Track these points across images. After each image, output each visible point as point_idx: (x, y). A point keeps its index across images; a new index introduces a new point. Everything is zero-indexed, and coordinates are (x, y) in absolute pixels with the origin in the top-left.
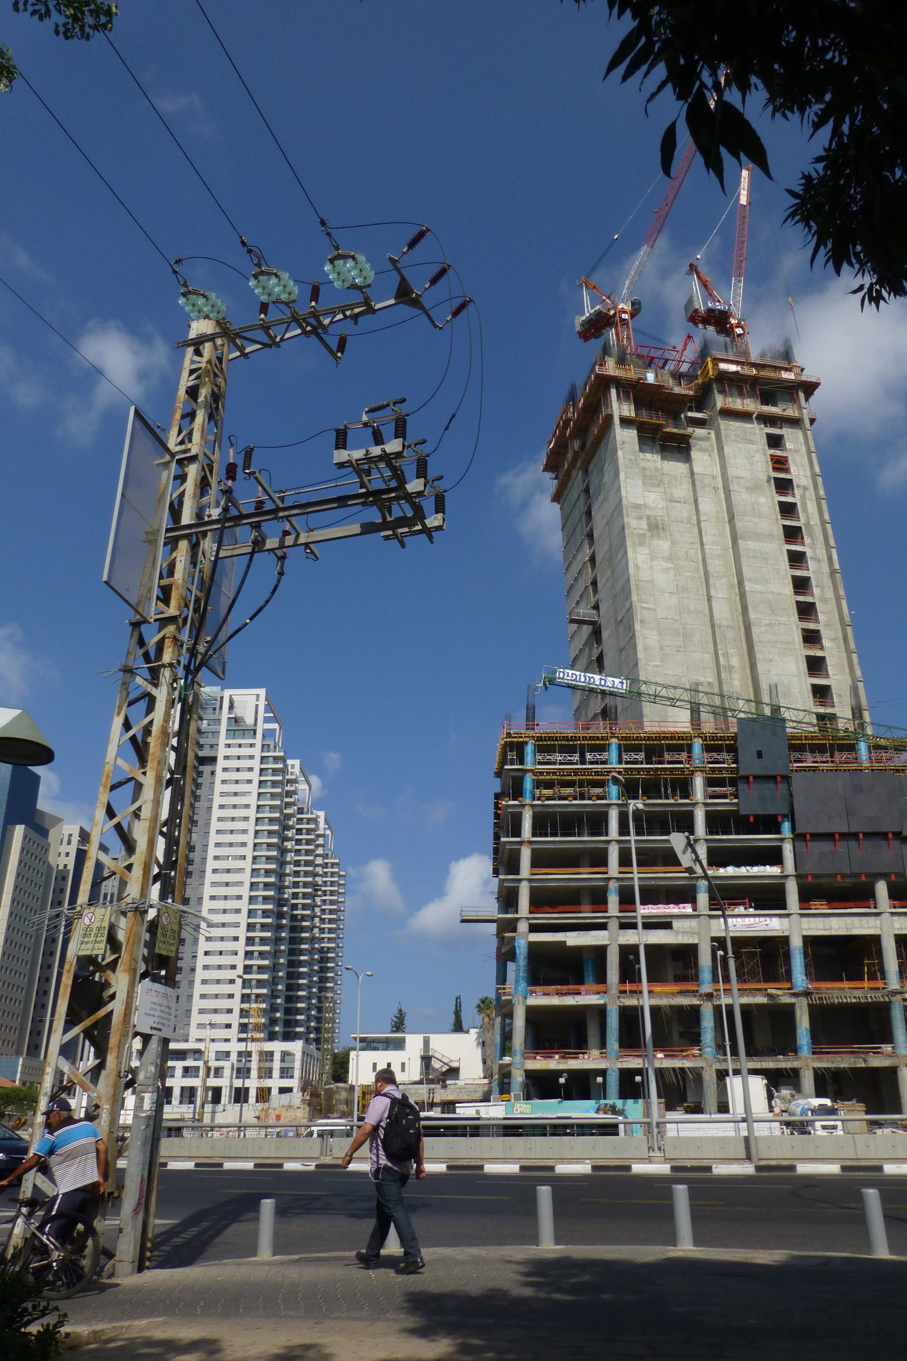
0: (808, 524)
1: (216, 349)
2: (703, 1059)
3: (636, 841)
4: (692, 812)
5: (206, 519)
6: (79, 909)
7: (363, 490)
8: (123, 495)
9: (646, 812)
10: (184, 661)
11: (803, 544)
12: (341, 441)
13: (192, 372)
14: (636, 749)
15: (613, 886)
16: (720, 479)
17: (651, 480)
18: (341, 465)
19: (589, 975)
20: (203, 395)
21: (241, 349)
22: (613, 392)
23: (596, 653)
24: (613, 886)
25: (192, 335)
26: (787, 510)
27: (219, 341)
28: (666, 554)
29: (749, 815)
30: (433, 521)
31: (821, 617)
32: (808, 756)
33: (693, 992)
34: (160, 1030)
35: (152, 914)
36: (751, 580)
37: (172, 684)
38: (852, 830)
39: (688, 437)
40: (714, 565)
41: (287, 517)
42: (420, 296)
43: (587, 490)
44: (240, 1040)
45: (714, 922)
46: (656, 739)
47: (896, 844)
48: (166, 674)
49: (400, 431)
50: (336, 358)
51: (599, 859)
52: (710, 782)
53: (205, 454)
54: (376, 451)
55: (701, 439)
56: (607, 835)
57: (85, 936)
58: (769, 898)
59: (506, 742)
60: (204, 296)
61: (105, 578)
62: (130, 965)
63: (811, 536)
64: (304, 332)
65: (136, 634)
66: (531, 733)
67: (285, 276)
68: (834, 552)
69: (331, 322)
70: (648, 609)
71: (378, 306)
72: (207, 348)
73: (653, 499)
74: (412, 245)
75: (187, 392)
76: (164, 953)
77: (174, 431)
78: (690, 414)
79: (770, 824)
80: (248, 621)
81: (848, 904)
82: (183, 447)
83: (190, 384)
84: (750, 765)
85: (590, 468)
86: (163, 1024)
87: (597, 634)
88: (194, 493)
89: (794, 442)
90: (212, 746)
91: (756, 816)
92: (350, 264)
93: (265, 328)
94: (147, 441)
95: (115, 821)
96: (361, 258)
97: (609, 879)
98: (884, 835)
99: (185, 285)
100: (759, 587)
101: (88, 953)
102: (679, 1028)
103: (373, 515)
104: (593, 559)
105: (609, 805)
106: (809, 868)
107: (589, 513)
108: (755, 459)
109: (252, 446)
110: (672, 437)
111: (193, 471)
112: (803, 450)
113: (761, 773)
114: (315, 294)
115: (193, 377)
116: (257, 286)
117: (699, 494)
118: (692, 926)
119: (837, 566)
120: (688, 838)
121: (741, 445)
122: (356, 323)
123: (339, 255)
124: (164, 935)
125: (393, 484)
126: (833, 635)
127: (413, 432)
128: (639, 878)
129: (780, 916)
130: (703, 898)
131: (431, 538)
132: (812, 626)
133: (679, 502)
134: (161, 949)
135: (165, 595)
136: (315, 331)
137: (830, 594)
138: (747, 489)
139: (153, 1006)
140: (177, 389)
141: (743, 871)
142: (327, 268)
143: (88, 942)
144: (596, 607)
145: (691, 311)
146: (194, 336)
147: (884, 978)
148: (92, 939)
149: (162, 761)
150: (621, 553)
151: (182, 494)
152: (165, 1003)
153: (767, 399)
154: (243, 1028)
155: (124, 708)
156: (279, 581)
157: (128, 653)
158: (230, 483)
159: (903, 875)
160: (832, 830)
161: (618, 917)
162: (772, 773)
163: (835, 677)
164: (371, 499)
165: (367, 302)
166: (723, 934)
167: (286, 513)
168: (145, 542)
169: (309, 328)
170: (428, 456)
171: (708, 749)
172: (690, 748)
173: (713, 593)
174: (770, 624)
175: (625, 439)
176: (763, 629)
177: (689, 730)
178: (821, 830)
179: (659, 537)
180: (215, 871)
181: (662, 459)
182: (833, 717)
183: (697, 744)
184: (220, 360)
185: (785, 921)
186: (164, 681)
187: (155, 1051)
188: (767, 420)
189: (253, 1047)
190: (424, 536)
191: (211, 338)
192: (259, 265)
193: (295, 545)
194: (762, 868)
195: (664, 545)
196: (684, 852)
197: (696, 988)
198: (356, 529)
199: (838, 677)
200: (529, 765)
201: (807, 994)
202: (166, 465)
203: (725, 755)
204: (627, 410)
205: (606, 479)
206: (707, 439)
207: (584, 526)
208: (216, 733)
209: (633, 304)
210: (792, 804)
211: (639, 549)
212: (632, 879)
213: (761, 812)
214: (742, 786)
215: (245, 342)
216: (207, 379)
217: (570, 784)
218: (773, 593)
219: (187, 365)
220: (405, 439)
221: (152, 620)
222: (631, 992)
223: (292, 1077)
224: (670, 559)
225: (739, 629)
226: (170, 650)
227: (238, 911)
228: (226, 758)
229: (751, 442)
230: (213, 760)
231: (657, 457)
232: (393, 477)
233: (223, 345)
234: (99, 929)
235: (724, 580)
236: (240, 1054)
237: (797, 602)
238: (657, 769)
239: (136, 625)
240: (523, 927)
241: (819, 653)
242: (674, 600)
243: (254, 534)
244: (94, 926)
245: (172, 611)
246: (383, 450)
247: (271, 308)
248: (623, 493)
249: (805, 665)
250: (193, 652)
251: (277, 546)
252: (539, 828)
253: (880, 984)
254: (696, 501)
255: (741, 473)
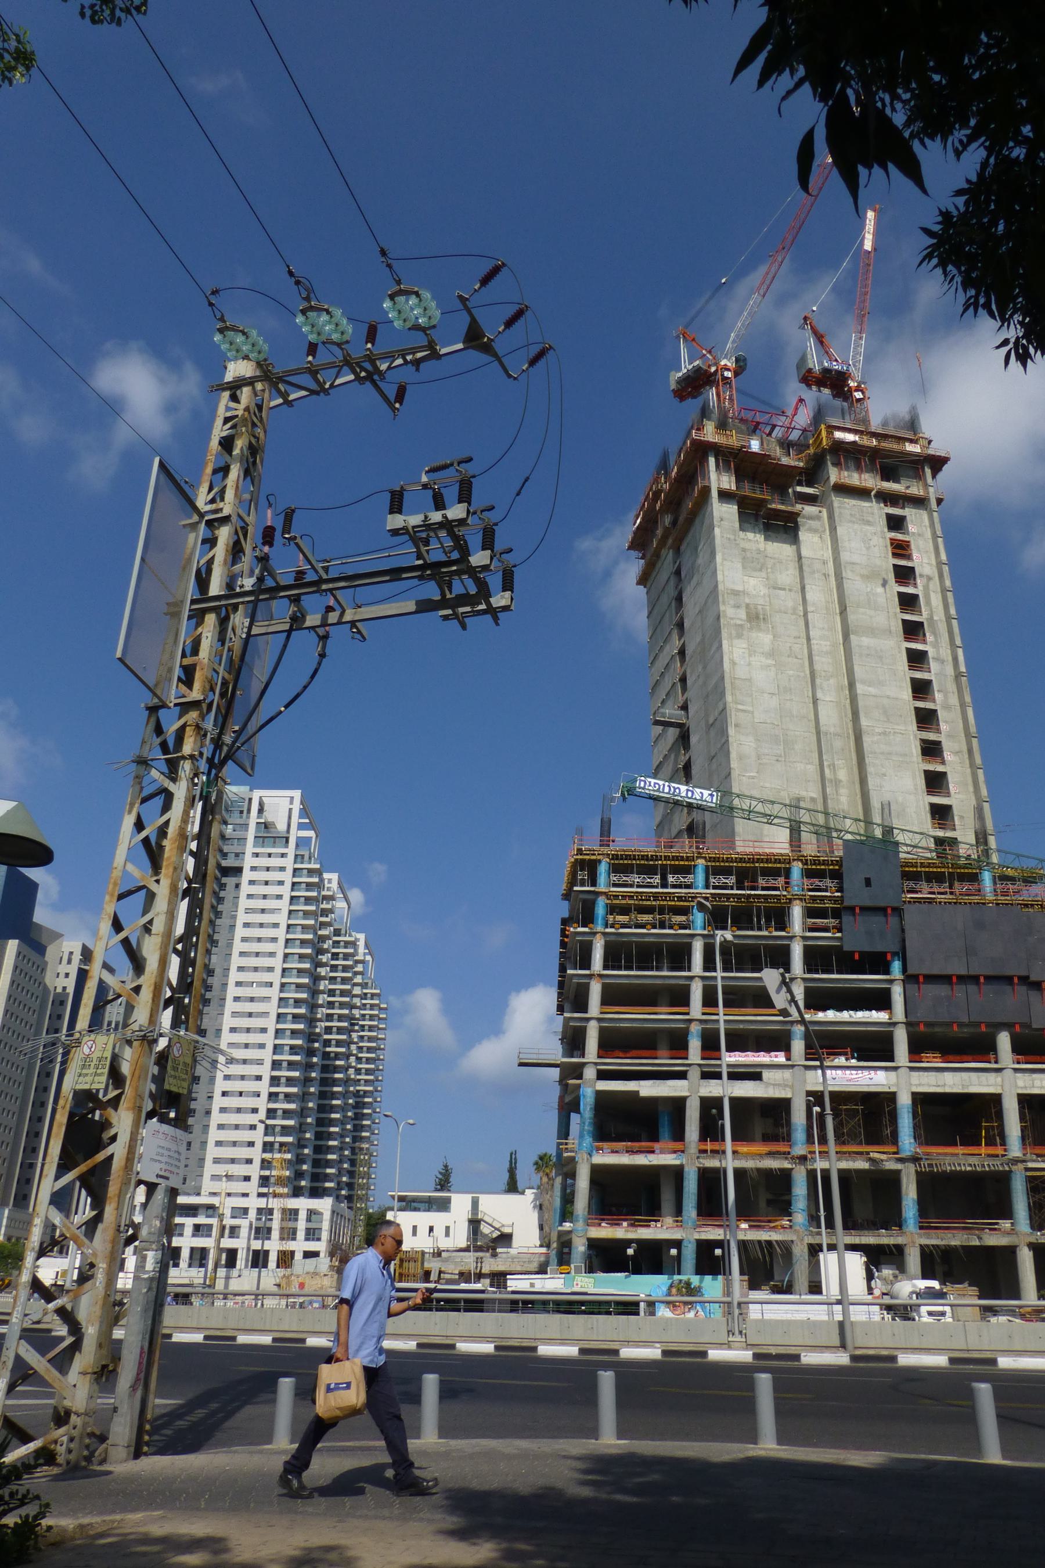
0: (931, 618)
1: (256, 395)
2: (793, 1230)
3: (723, 978)
4: (789, 945)
5: (238, 590)
6: (77, 1035)
7: (420, 562)
8: (143, 559)
9: (735, 945)
10: (207, 752)
11: (924, 642)
12: (397, 504)
13: (227, 420)
14: (726, 872)
15: (695, 1029)
16: (831, 564)
17: (752, 563)
18: (395, 532)
19: (665, 1131)
20: (239, 447)
21: (284, 395)
22: (712, 461)
23: (683, 759)
24: (695, 1029)
25: (229, 377)
26: (908, 602)
27: (259, 386)
28: (767, 649)
29: (853, 953)
30: (500, 599)
31: (943, 727)
32: (924, 886)
33: (784, 1153)
34: (167, 1178)
35: (163, 1043)
36: (863, 682)
37: (192, 779)
38: (972, 973)
39: (798, 514)
40: (822, 663)
41: (331, 590)
42: (492, 340)
43: (678, 573)
44: (260, 1195)
45: (810, 1074)
46: (749, 861)
47: (1021, 990)
48: (186, 767)
49: (465, 495)
50: (394, 409)
51: (680, 997)
52: (810, 913)
53: (239, 516)
54: (436, 517)
55: (811, 518)
56: (689, 970)
57: (83, 1067)
58: (873, 1048)
59: (576, 860)
60: (244, 333)
61: (119, 654)
62: (135, 1103)
63: (934, 633)
64: (358, 378)
65: (153, 719)
66: (606, 850)
67: (338, 312)
68: (960, 652)
69: (389, 368)
70: (743, 711)
71: (443, 351)
72: (245, 394)
73: (754, 585)
74: (485, 281)
75: (220, 443)
76: (174, 1089)
77: (204, 489)
78: (799, 489)
79: (878, 963)
80: (283, 709)
81: (965, 1057)
82: (213, 506)
83: (224, 434)
84: (856, 895)
85: (682, 548)
86: (171, 1172)
87: (684, 738)
88: (225, 561)
89: (917, 522)
90: (237, 855)
91: (860, 952)
92: (413, 301)
93: (313, 372)
94: (171, 497)
95: (122, 935)
96: (426, 295)
97: (690, 1021)
98: (1008, 980)
99: (222, 319)
100: (872, 690)
101: (87, 1087)
102: (767, 1194)
103: (431, 591)
104: (682, 652)
105: (693, 936)
106: (921, 1015)
107: (679, 599)
108: (872, 543)
109: (293, 507)
110: (777, 514)
111: (224, 534)
112: (928, 534)
113: (868, 903)
114: (372, 334)
115: (229, 425)
116: (305, 324)
117: (806, 581)
118: (784, 1078)
119: (963, 669)
120: (782, 975)
121: (856, 526)
122: (417, 370)
123: (400, 290)
124: (175, 1069)
125: (455, 555)
126: (956, 747)
127: (479, 499)
128: (725, 1021)
130: (798, 1046)
131: (496, 620)
132: (932, 736)
133: (784, 589)
134: (171, 1085)
135: (188, 677)
136: (369, 377)
137: (954, 700)
138: (862, 576)
139: (161, 1151)
140: (210, 439)
141: (845, 1016)
142: (387, 304)
143: (87, 1075)
144: (685, 707)
145: (804, 371)
146: (231, 379)
147: (1003, 1143)
148: (92, 1070)
149: (179, 868)
150: (714, 648)
151: (211, 562)
152: (174, 1147)
153: (888, 474)
154: (264, 1181)
155: (137, 805)
156: (319, 664)
157: (144, 742)
158: (266, 549)
159: (1028, 1026)
160: (949, 971)
161: (699, 1065)
162: (883, 904)
163: (957, 796)
164: (428, 572)
165: (431, 346)
166: (821, 1088)
167: (331, 586)
168: (166, 614)
169: (363, 374)
170: (496, 524)
171: (809, 874)
172: (787, 873)
173: (819, 695)
174: (884, 733)
175: (724, 515)
176: (875, 738)
177: (787, 851)
178: (935, 971)
179: (760, 630)
180: (237, 999)
181: (766, 539)
182: (953, 842)
183: (797, 868)
184: (260, 407)
185: (892, 1075)
186: (183, 775)
187: (160, 1202)
188: (887, 498)
189: (275, 1204)
190: (488, 617)
191: (250, 382)
192: (308, 299)
193: (339, 623)
194: (867, 1013)
195: (764, 639)
196: (778, 991)
197: (787, 1150)
198: (411, 606)
199: (960, 796)
200: (602, 887)
201: (915, 1159)
202: (194, 526)
203: (828, 883)
204: (727, 481)
205: (700, 561)
206: (819, 518)
207: (674, 612)
208: (243, 840)
209: (737, 360)
210: (904, 941)
211: (736, 642)
212: (718, 1021)
213: (867, 948)
214: (847, 919)
215: (289, 388)
216: (244, 429)
217: (649, 910)
218: (888, 697)
219: (221, 412)
220: (469, 504)
221: (172, 705)
222: (712, 1151)
223: (319, 1239)
224: (772, 654)
225: (848, 737)
226: (192, 739)
227: (262, 1046)
228: (253, 869)
229: (868, 523)
230: (239, 870)
231: (760, 538)
232: (454, 548)
233: (263, 391)
234: (100, 1059)
235: (832, 681)
236: (260, 1211)
237: (917, 709)
238: (750, 896)
239: (153, 710)
240: (590, 1073)
241: (940, 768)
242: (774, 702)
243: (293, 608)
244: (95, 1056)
245: (196, 694)
246: (445, 517)
247: (321, 348)
248: (720, 577)
249: (923, 781)
250: (217, 743)
251: (318, 623)
252: (612, 959)
253: (1000, 1151)
254: (803, 588)
255: (856, 558)
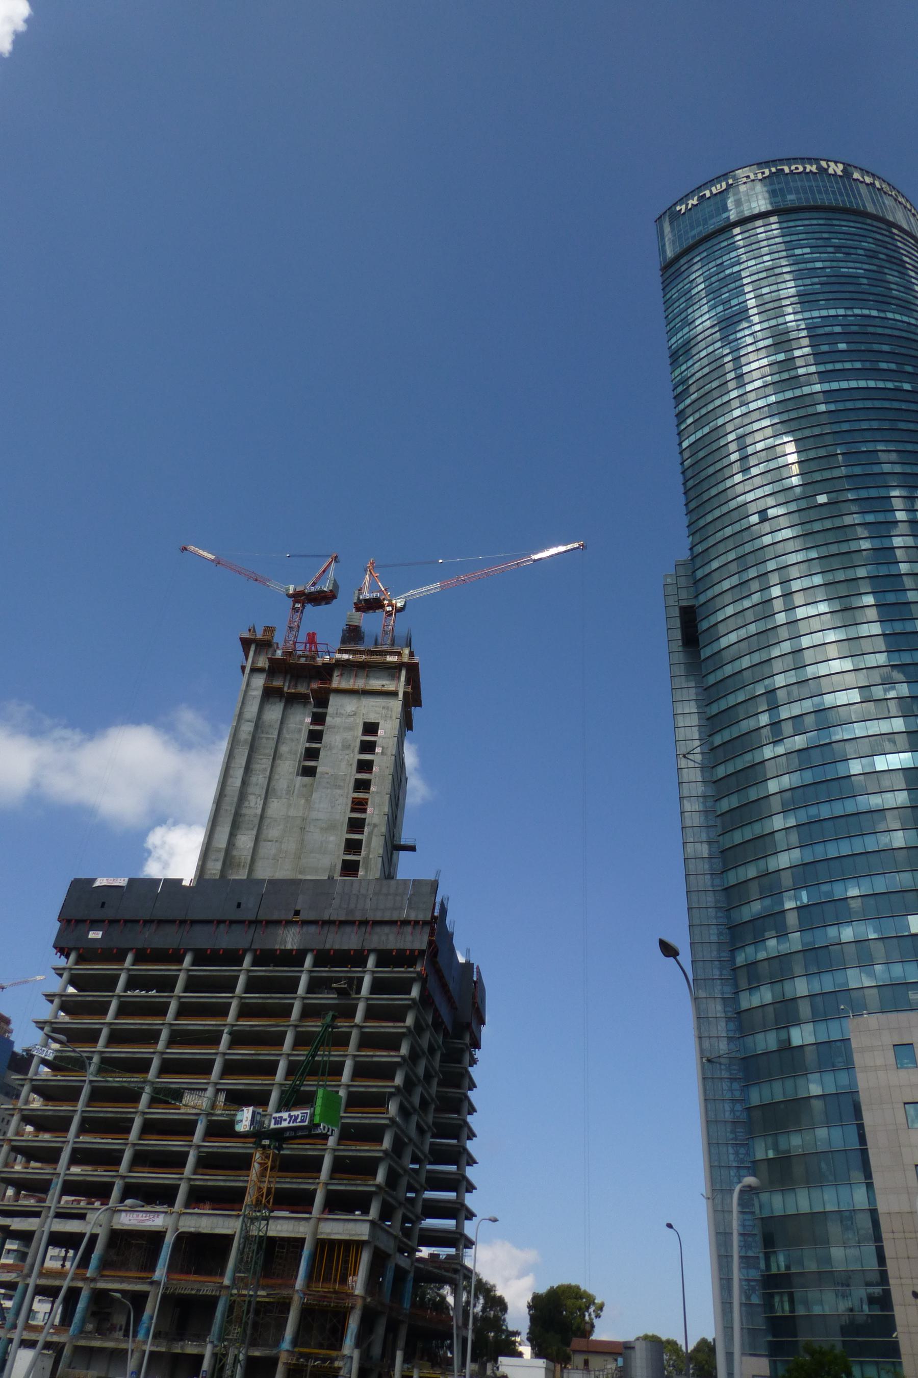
0: (367, 858)
129: (166, 1213)
138: (322, 829)
229: (339, 787)
253: (218, 1280)
